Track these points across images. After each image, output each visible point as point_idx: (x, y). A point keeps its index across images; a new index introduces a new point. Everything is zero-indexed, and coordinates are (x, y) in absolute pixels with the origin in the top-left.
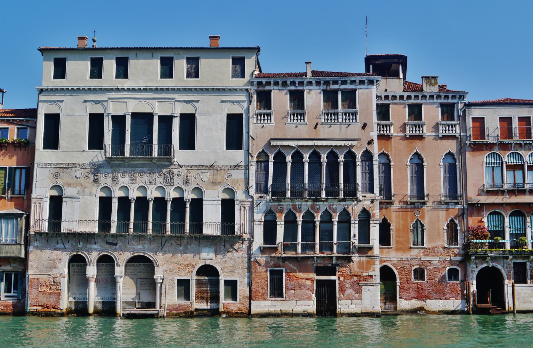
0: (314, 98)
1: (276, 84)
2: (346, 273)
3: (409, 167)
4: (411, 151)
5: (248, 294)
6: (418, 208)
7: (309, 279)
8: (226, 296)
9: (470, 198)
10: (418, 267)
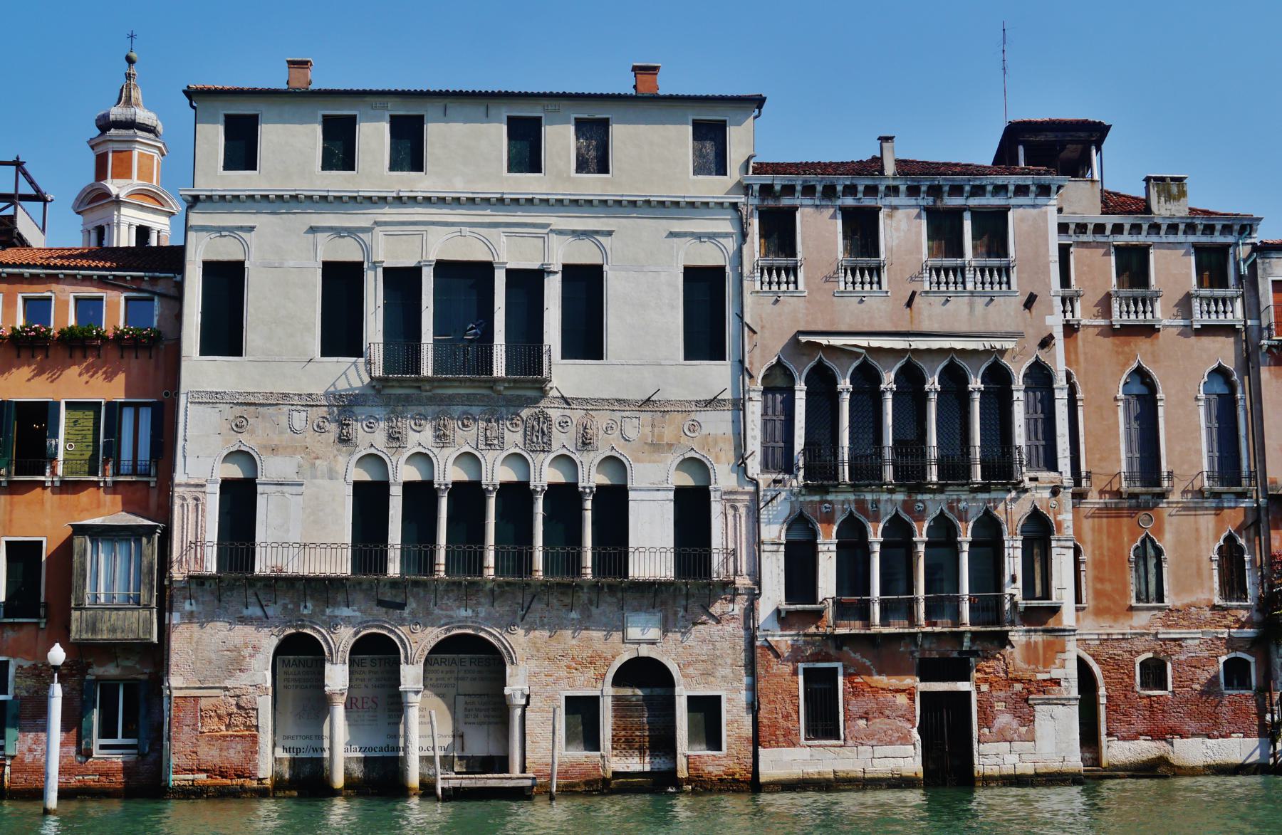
0: (903, 231)
1: (809, 191)
2: (995, 673)
3: (1121, 403)
4: (1126, 364)
5: (748, 731)
6: (1147, 508)
7: (904, 691)
8: (693, 739)
9: (1274, 482)
10: (1150, 655)
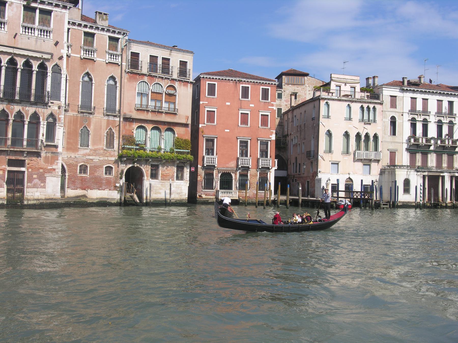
4: (84, 71)
